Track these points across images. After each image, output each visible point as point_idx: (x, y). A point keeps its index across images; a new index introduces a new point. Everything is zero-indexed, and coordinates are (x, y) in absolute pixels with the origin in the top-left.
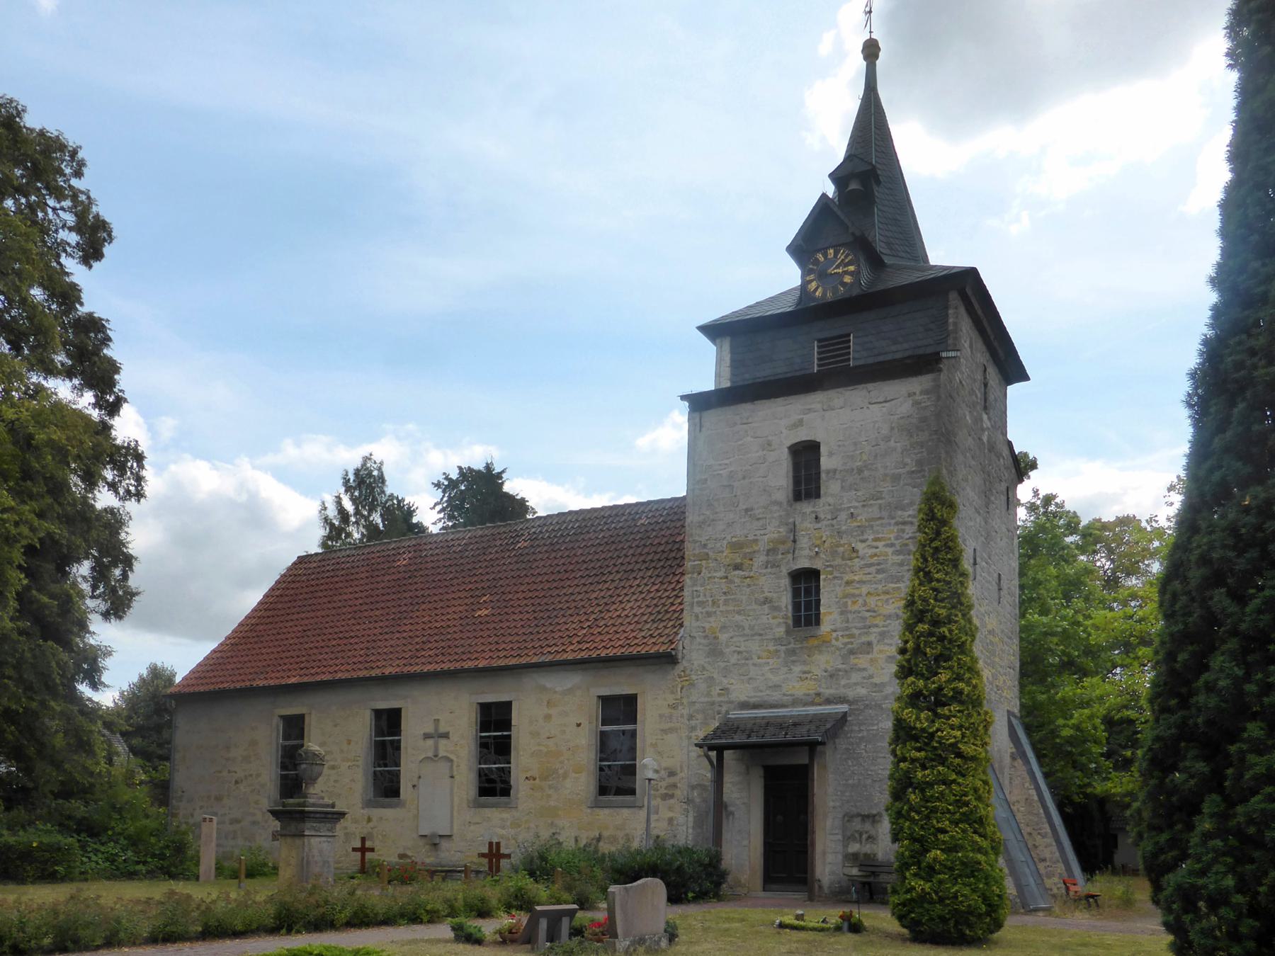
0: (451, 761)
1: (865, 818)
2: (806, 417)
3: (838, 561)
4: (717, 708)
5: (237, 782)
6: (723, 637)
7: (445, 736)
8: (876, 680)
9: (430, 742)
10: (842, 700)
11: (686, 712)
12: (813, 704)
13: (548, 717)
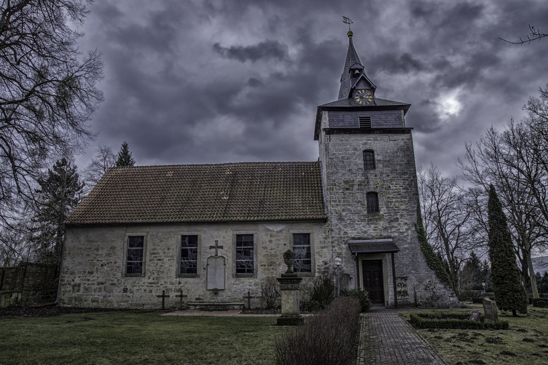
0: (224, 258)
1: (402, 278)
2: (369, 142)
3: (384, 190)
4: (343, 239)
5: (102, 265)
6: (344, 214)
7: (222, 247)
8: (401, 231)
9: (213, 250)
10: (389, 237)
11: (330, 240)
12: (379, 238)
13: (271, 241)
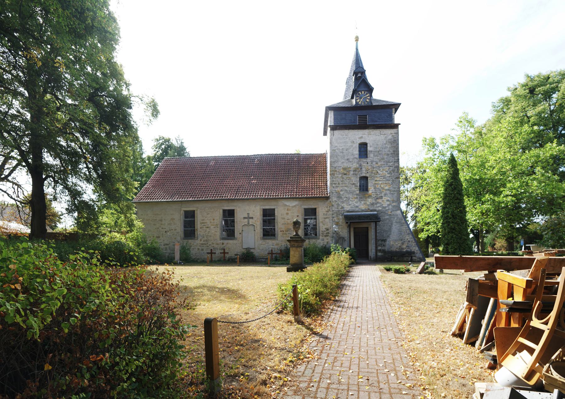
1: (382, 240)
6: (341, 193)
7: (252, 218)
9: (246, 220)
10: (375, 211)
13: (287, 214)
